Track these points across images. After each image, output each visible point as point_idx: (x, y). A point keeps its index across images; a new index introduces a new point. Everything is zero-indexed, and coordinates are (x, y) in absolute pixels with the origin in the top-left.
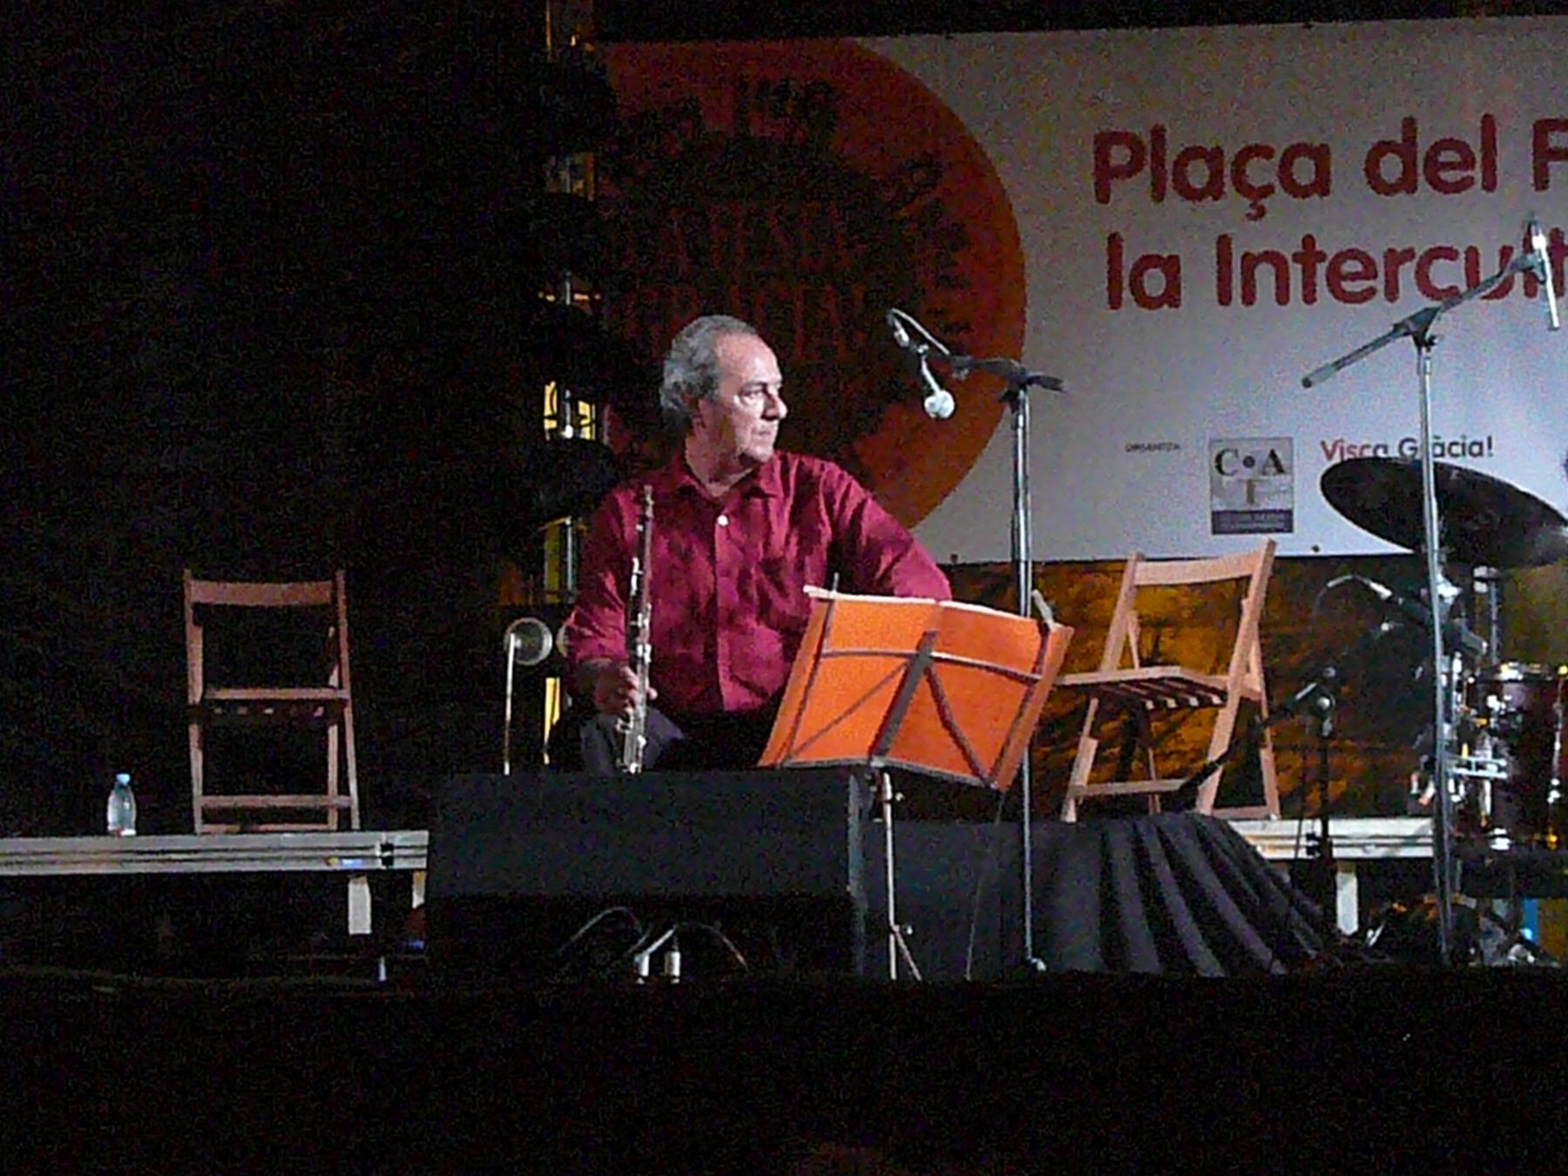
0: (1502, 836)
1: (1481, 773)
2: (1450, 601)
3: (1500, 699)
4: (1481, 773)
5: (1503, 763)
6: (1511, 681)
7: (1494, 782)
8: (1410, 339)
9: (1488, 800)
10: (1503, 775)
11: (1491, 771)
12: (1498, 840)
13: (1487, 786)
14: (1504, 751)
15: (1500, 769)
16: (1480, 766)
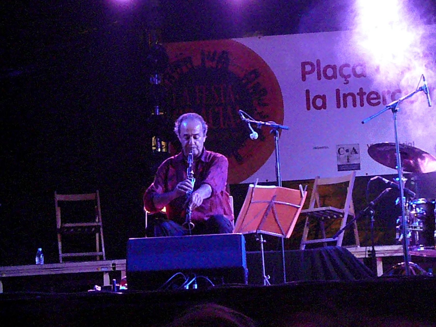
0: (422, 247)
1: (416, 229)
2: (405, 182)
3: (420, 209)
4: (416, 229)
5: (422, 226)
6: (422, 204)
7: (419, 231)
8: (391, 110)
9: (418, 237)
10: (422, 230)
11: (418, 229)
12: (421, 248)
13: (417, 233)
14: (421, 223)
15: (421, 228)
16: (415, 227)
